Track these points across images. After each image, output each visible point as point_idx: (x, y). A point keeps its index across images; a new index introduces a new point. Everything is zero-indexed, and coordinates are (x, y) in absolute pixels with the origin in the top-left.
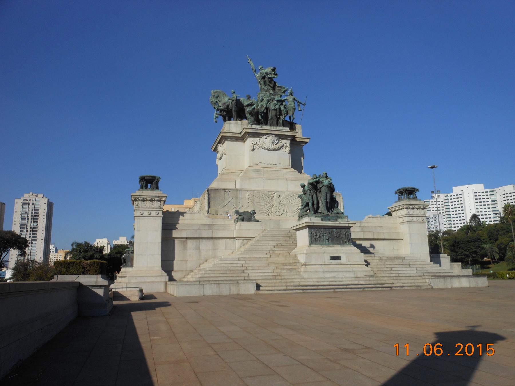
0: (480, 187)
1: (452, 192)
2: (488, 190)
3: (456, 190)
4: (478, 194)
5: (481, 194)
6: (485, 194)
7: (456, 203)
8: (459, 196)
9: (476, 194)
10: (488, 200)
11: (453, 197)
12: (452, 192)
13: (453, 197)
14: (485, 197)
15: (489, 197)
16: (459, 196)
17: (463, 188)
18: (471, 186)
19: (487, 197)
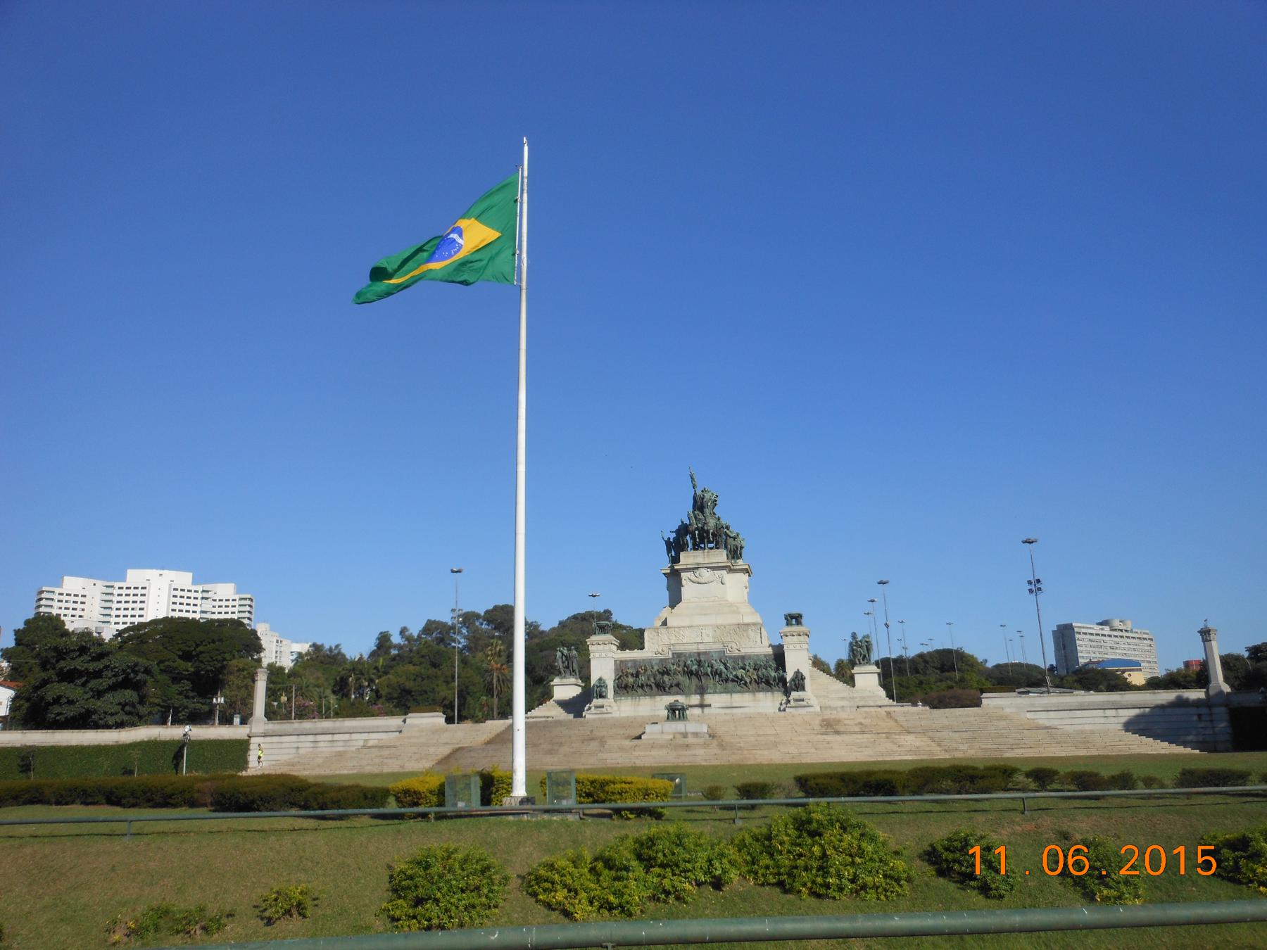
0: (184, 579)
1: (124, 580)
2: (200, 588)
3: (135, 577)
4: (179, 593)
5: (186, 594)
6: (192, 595)
7: (130, 606)
8: (140, 591)
9: (175, 593)
10: (195, 608)
11: (124, 592)
12: (124, 580)
13: (124, 592)
14: (192, 601)
15: (198, 602)
16: (140, 591)
17: (152, 574)
18: (169, 575)
19: (195, 602)
